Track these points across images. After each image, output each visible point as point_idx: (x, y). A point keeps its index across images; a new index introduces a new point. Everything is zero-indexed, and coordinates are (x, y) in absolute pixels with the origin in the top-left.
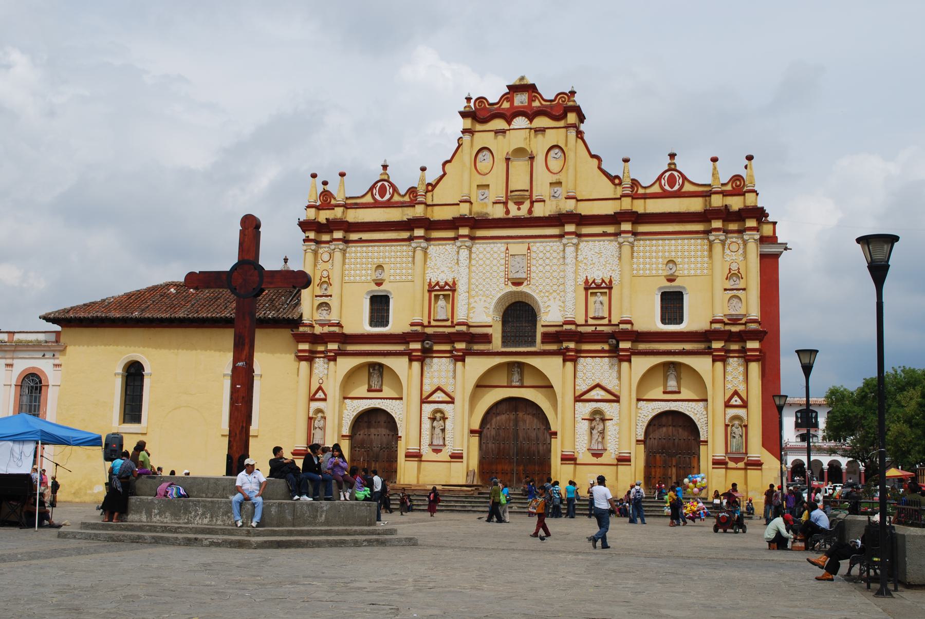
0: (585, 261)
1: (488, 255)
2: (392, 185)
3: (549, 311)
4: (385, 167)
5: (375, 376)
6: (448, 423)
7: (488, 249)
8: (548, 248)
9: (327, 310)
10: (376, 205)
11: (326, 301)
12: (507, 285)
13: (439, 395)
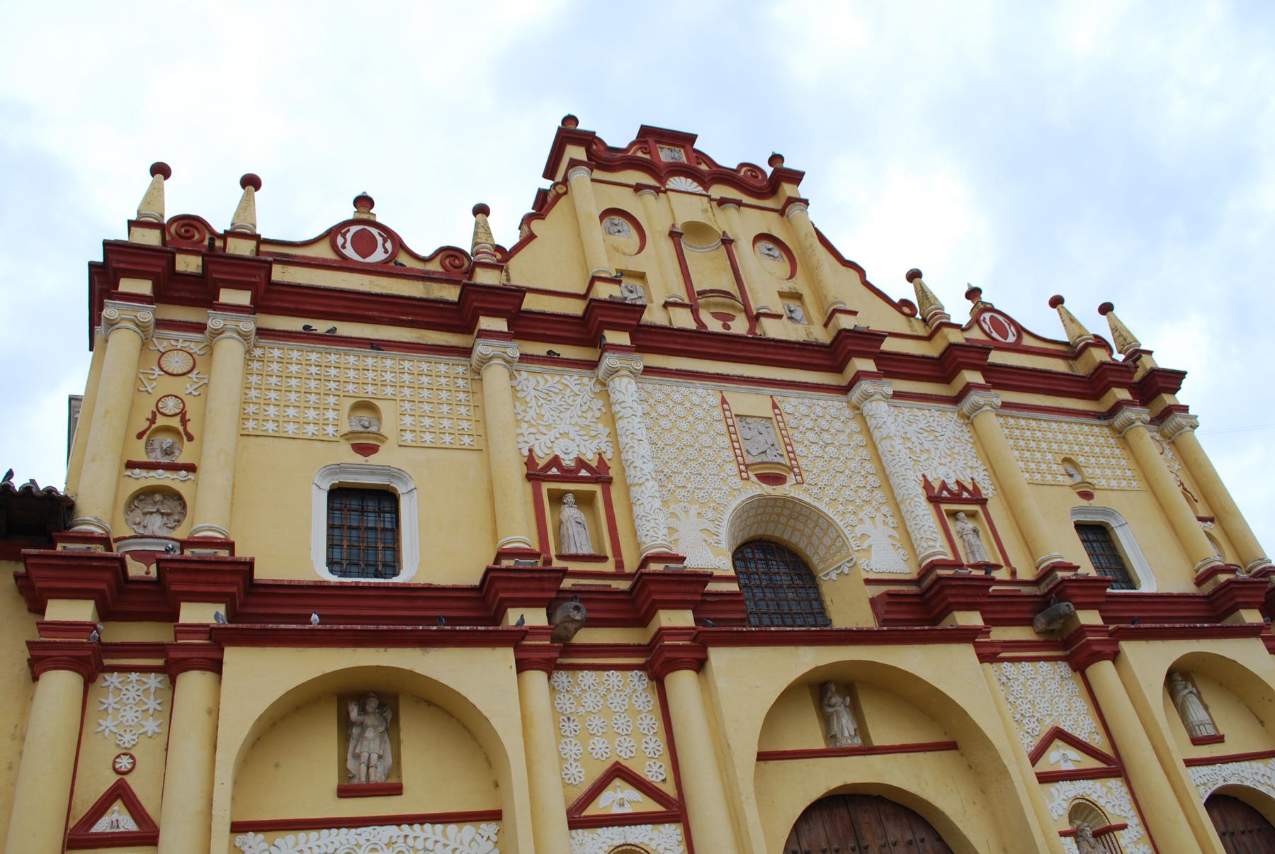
1: (680, 410)
2: (389, 234)
3: (870, 546)
5: (370, 734)
7: (677, 397)
8: (819, 411)
9: (168, 515)
10: (344, 265)
12: (748, 479)
13: (620, 795)
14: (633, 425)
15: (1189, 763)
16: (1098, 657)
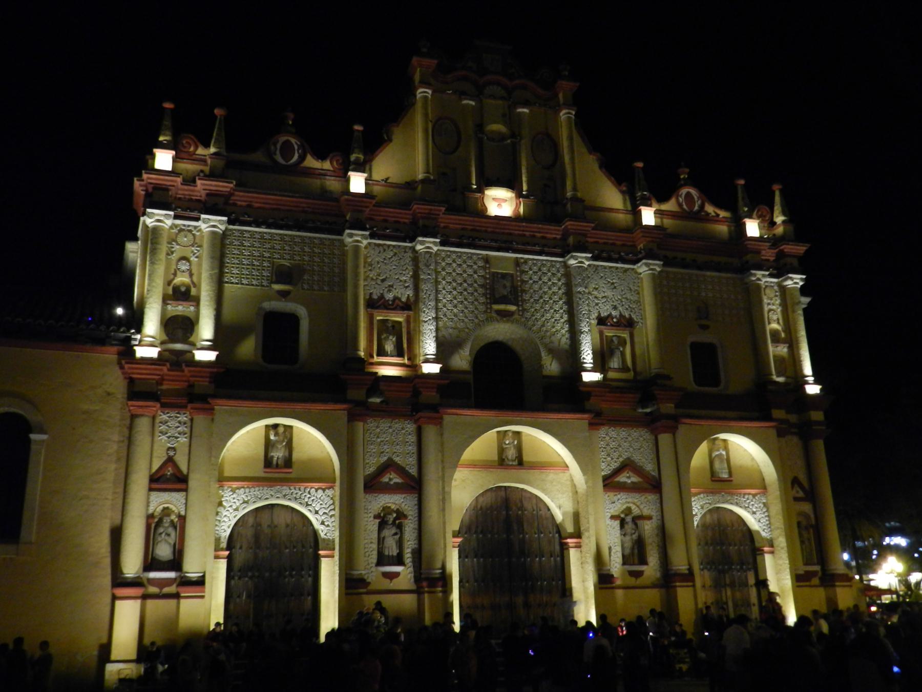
0: (595, 293)
1: (459, 270)
5: (280, 446)
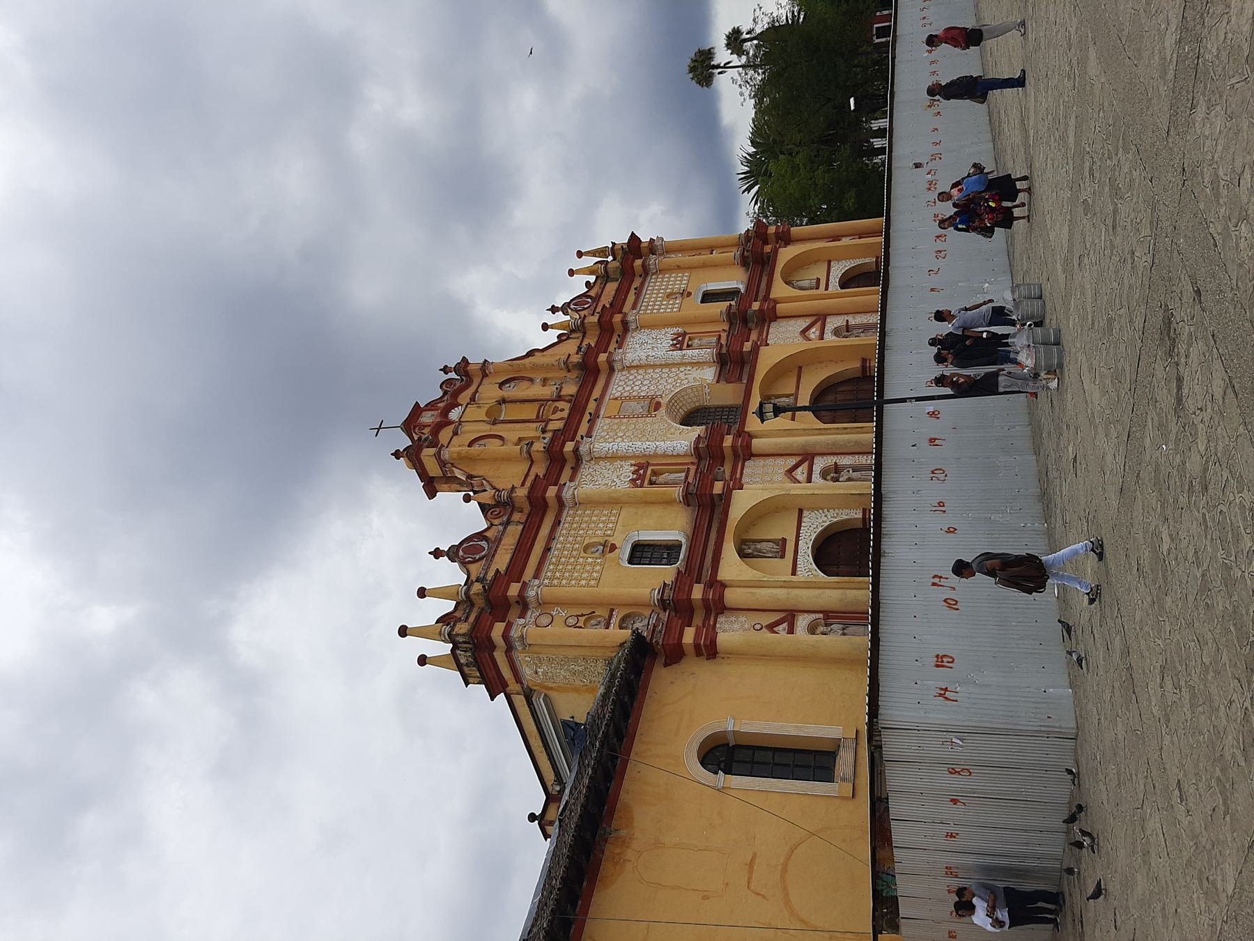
4: (437, 553)
6: (845, 461)
11: (620, 616)
14: (622, 446)
15: (827, 289)
16: (774, 308)
